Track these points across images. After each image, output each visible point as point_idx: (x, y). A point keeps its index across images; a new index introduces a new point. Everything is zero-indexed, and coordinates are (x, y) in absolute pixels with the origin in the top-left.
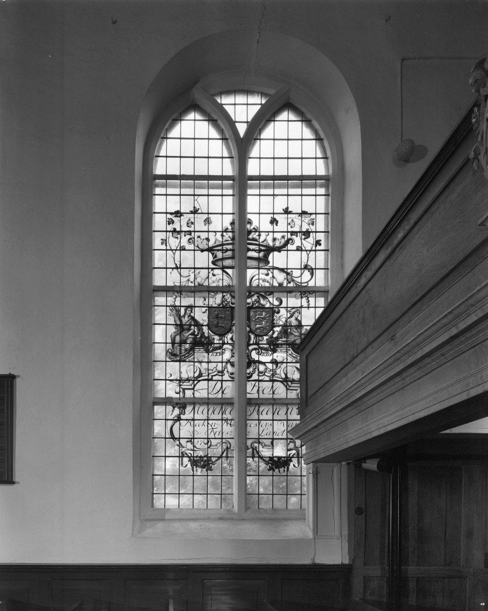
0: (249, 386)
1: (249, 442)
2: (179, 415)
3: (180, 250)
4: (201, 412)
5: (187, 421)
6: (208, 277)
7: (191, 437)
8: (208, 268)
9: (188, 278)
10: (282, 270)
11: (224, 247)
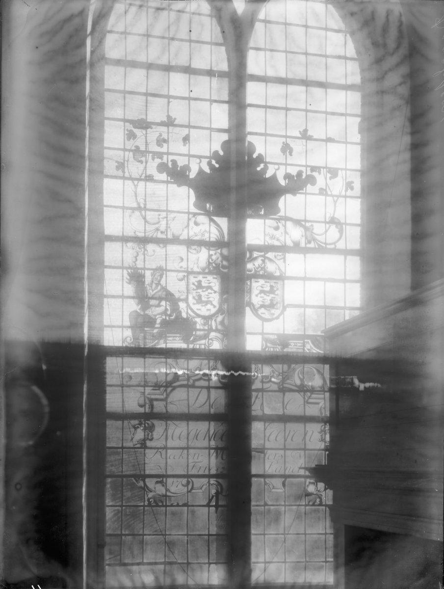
2: (144, 440)
5: (156, 450)
6: (188, 224)
9: (157, 226)
10: (297, 222)
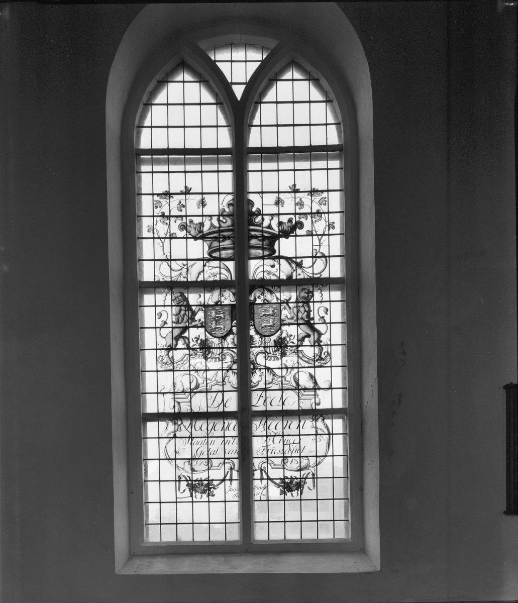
0: (255, 396)
1: (257, 463)
2: (175, 431)
3: (171, 238)
8: (203, 260)
9: (180, 272)
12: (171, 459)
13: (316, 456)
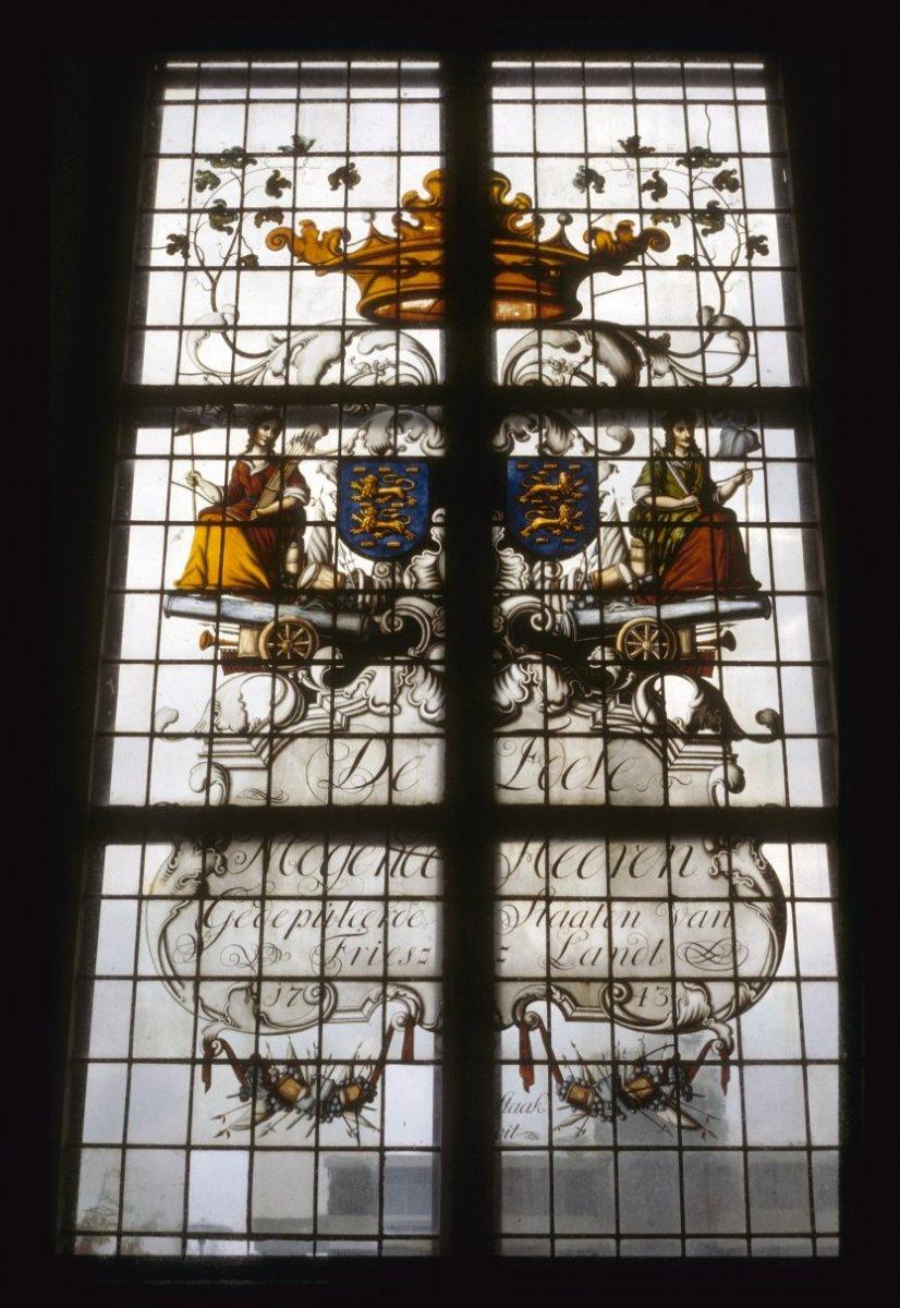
1: (509, 994)
2: (205, 873)
3: (238, 268)
4: (298, 868)
7: (246, 972)
11: (403, 256)
12: (179, 979)
13: (737, 980)
